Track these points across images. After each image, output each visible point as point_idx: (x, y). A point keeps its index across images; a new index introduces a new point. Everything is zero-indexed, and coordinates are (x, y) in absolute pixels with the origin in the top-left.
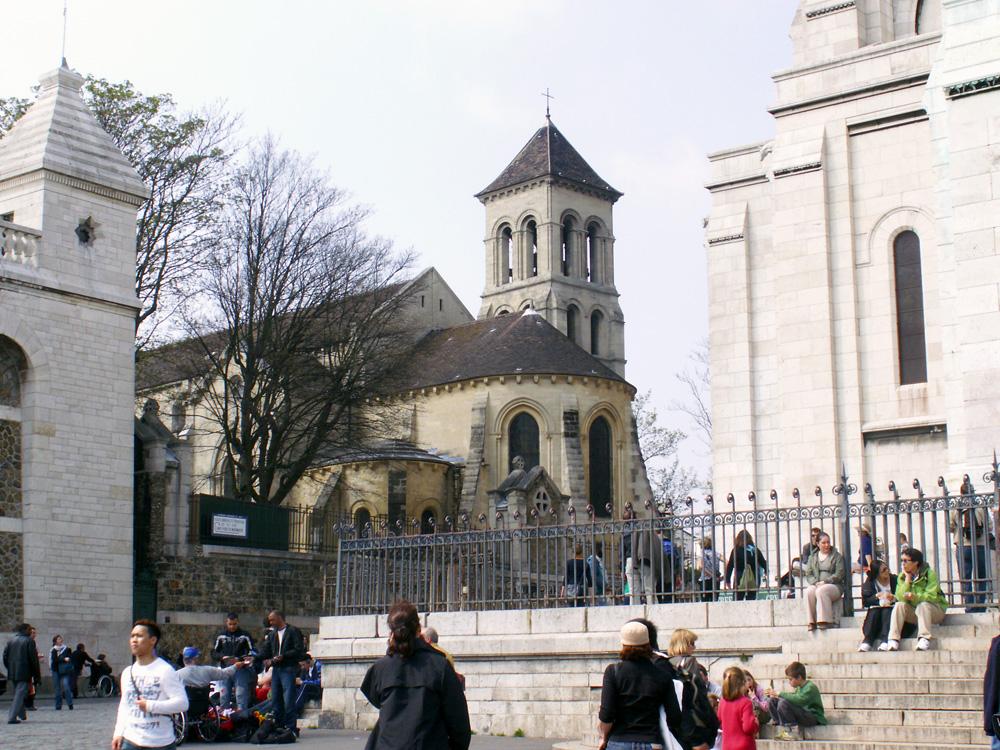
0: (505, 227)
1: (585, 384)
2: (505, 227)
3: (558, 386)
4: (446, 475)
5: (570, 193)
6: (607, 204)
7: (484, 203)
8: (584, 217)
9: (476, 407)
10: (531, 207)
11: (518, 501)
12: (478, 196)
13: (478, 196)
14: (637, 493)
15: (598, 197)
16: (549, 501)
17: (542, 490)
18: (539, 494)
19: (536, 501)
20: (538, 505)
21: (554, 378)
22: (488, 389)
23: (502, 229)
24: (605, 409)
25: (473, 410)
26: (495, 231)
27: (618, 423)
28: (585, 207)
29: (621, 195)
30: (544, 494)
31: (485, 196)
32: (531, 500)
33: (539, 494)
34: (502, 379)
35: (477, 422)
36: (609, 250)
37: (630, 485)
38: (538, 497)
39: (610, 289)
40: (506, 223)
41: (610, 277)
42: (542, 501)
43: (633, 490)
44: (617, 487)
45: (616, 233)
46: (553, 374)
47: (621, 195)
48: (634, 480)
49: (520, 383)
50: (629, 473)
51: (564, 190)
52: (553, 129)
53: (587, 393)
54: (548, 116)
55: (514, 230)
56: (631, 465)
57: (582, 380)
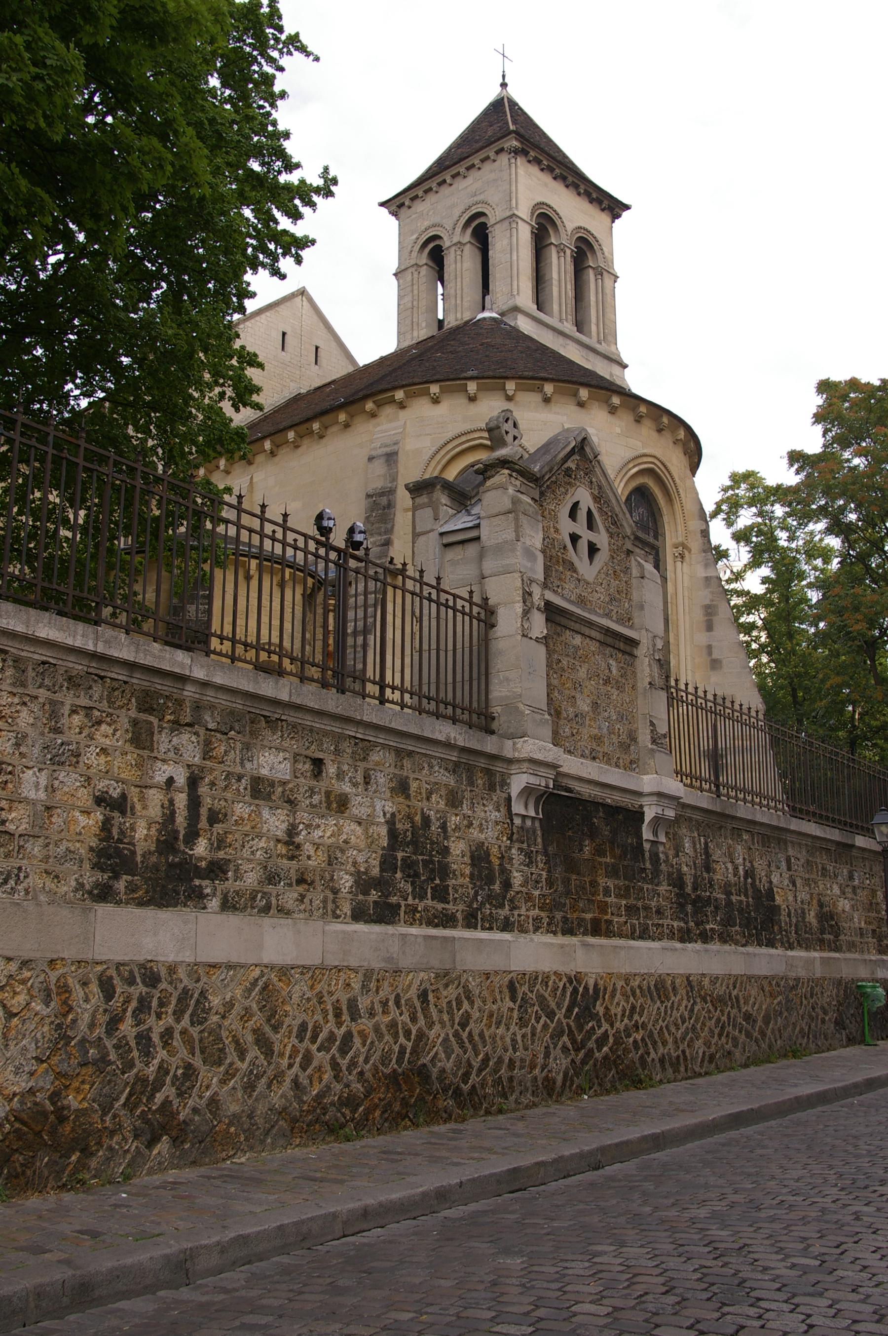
0: (431, 245)
1: (613, 410)
2: (431, 245)
3: (554, 407)
4: (309, 599)
5: (546, 178)
6: (605, 218)
7: (395, 214)
8: (570, 226)
9: (374, 453)
10: (475, 199)
11: (515, 502)
12: (382, 204)
13: (382, 204)
14: (715, 656)
15: (591, 202)
16: (602, 539)
17: (584, 496)
18: (575, 506)
19: (567, 526)
20: (574, 538)
21: (549, 388)
22: (402, 414)
23: (427, 250)
24: (650, 472)
25: (371, 459)
26: (414, 254)
27: (677, 506)
28: (573, 212)
29: (627, 207)
30: (590, 513)
31: (396, 205)
32: (555, 518)
33: (575, 506)
34: (434, 389)
35: (378, 484)
36: (608, 291)
37: (702, 638)
38: (573, 514)
39: (613, 353)
40: (436, 237)
41: (609, 334)
42: (586, 535)
43: (709, 647)
44: (677, 636)
45: (618, 267)
46: (546, 380)
47: (627, 207)
48: (710, 627)
49: (472, 399)
50: (699, 615)
51: (534, 170)
52: (513, 104)
53: (618, 430)
54: (504, 85)
55: (446, 243)
56: (704, 596)
57: (607, 401)
